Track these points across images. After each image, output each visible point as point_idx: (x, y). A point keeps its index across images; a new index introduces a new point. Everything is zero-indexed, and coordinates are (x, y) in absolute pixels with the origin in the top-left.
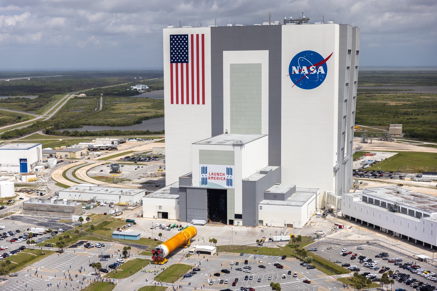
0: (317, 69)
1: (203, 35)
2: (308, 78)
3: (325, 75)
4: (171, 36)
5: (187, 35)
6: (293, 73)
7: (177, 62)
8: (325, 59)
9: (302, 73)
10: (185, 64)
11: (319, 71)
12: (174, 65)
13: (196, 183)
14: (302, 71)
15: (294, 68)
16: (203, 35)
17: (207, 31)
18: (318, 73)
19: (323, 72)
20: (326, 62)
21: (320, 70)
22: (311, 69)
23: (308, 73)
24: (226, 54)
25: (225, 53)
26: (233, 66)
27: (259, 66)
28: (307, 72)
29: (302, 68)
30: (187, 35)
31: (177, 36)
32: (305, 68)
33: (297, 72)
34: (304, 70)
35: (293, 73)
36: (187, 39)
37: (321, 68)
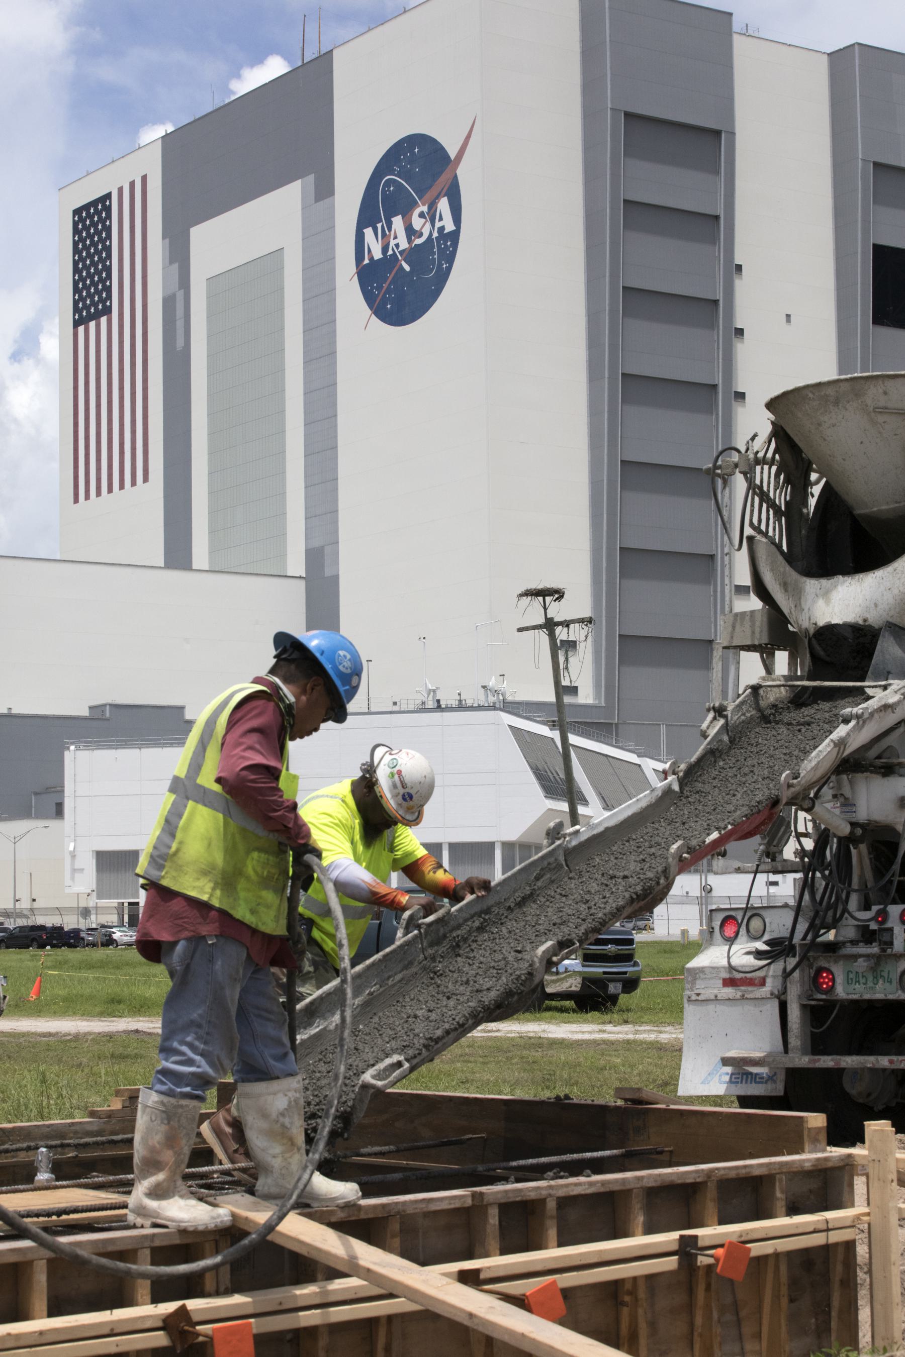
0: (432, 216)
1: (144, 179)
2: (407, 268)
3: (454, 236)
5: (108, 196)
6: (366, 261)
7: (91, 317)
8: (453, 156)
9: (390, 252)
11: (438, 224)
12: (81, 329)
14: (393, 243)
15: (368, 232)
16: (144, 179)
18: (435, 235)
19: (450, 227)
20: (459, 172)
21: (441, 219)
23: (404, 245)
28: (404, 245)
29: (390, 225)
30: (108, 196)
31: (86, 207)
32: (398, 222)
33: (378, 255)
34: (395, 237)
35: (366, 261)
36: (108, 210)
37: (443, 205)
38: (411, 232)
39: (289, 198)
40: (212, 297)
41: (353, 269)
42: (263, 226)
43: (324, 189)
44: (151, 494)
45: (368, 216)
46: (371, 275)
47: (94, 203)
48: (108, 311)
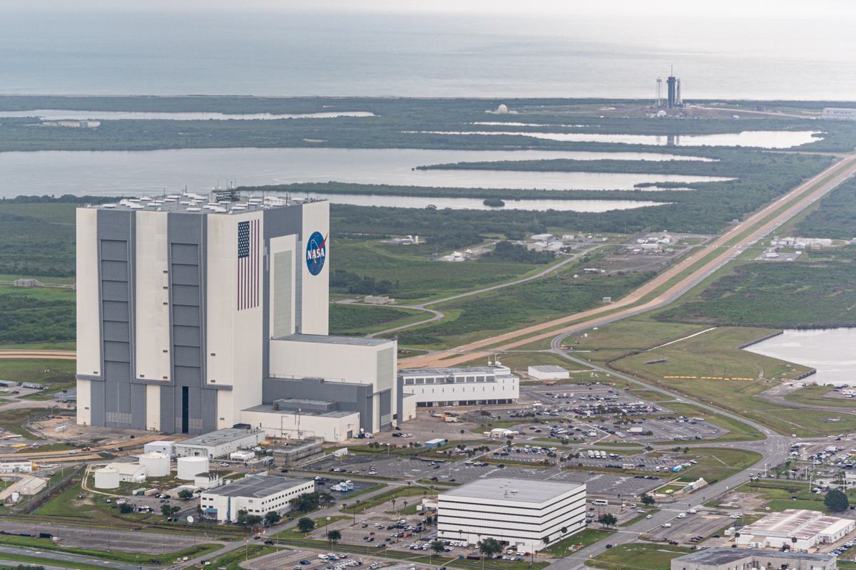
0: (320, 251)
4: (239, 223)
5: (249, 222)
10: (247, 258)
12: (240, 259)
13: (375, 391)
17: (259, 215)
22: (318, 252)
24: (271, 239)
25: (271, 239)
26: (276, 254)
27: (290, 252)
30: (249, 222)
31: (242, 223)
32: (314, 251)
37: (322, 249)
38: (317, 255)
39: (293, 237)
40: (275, 258)
41: (305, 259)
42: (284, 244)
43: (300, 238)
44: (260, 309)
45: (308, 248)
46: (310, 262)
47: (245, 223)
48: (248, 256)
